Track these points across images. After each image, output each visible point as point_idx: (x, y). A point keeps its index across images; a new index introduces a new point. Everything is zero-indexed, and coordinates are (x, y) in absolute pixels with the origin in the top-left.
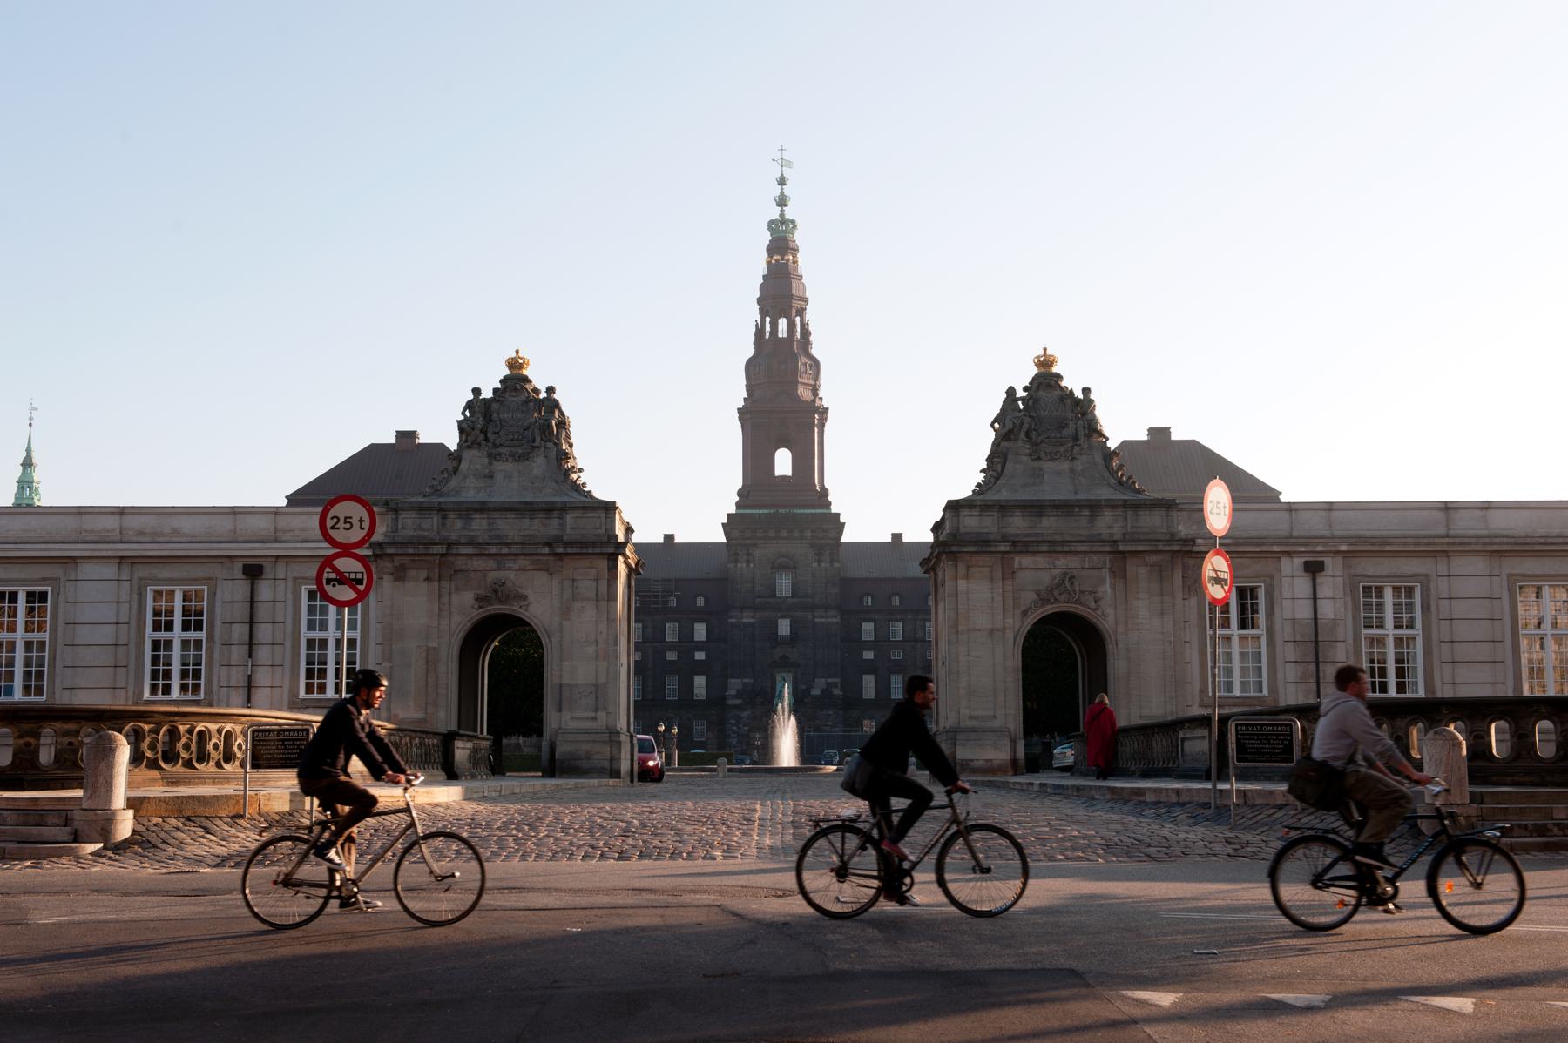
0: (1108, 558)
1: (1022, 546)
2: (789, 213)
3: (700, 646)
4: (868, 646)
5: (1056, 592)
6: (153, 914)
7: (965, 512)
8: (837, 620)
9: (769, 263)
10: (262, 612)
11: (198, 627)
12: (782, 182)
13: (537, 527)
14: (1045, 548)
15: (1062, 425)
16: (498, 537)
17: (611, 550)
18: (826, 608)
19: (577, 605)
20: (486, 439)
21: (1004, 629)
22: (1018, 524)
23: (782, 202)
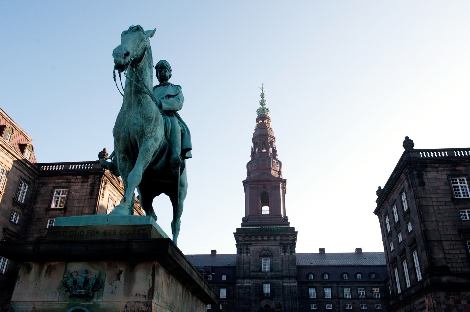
8: (296, 284)
9: (257, 125)
18: (290, 277)
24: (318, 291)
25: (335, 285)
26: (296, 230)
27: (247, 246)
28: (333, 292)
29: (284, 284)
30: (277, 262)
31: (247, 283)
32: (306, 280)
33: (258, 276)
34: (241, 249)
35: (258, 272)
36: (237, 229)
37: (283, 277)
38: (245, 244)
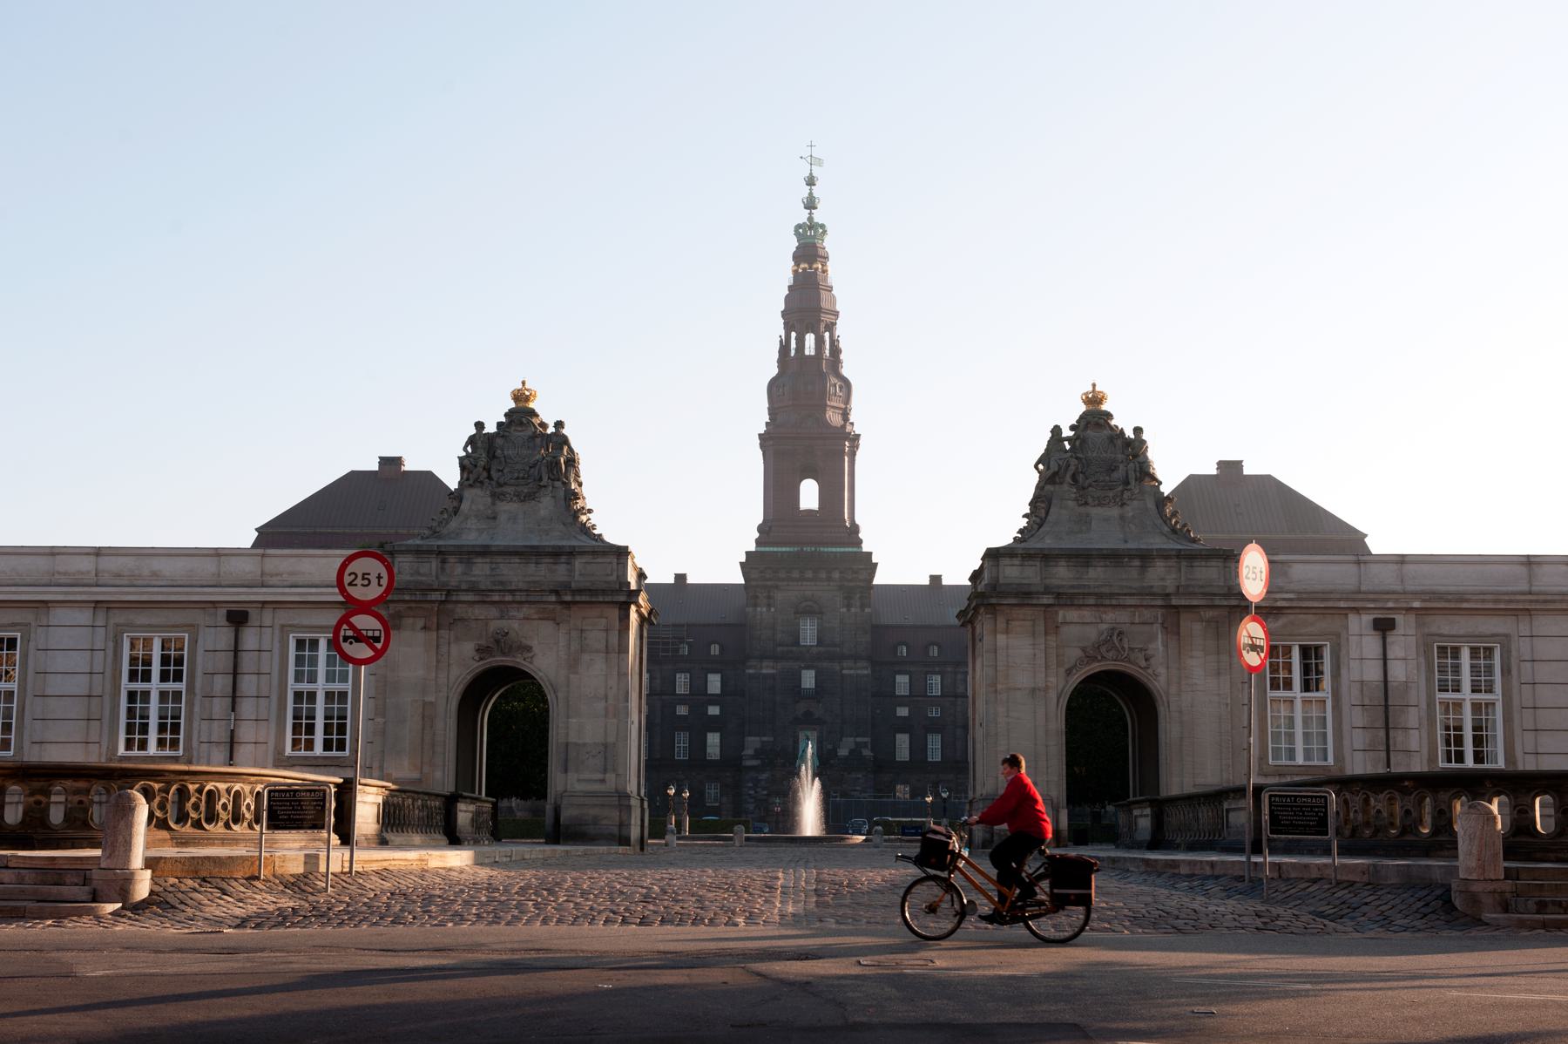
0: (1160, 612)
1: (1065, 598)
2: (818, 217)
3: (714, 700)
4: (902, 701)
5: (1103, 649)
6: (195, 968)
7: (1006, 561)
9: (795, 272)
10: (247, 662)
11: (178, 677)
12: (811, 181)
13: (542, 573)
14: (1091, 601)
15: (1112, 469)
16: (501, 583)
17: (622, 598)
18: (856, 658)
19: (586, 657)
20: (490, 477)
21: (1046, 689)
22: (1062, 574)
23: (810, 204)
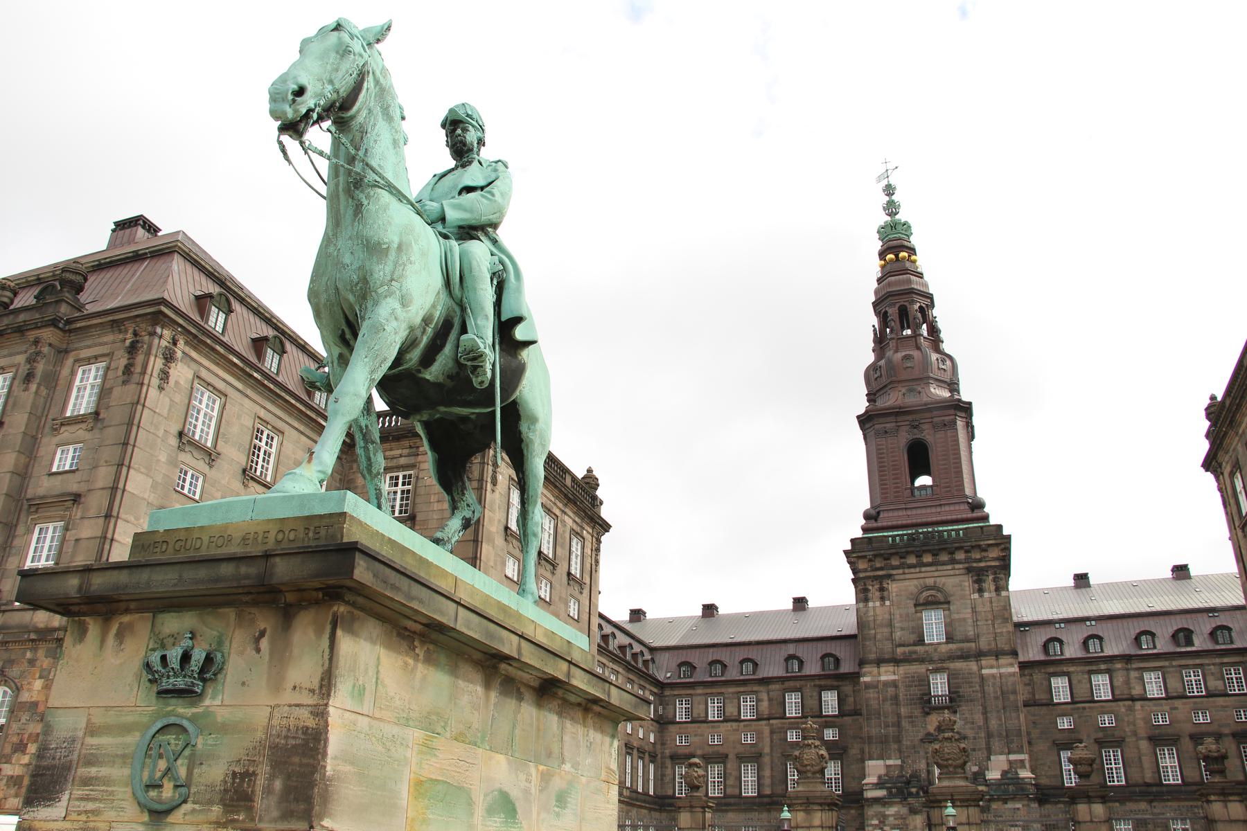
3: (829, 722)
9: (883, 267)
18: (998, 654)
24: (1074, 682)
25: (1119, 666)
26: (1005, 533)
27: (881, 583)
28: (1116, 684)
29: (984, 671)
30: (962, 616)
31: (887, 674)
32: (1042, 657)
33: (914, 656)
34: (866, 590)
35: (915, 644)
36: (853, 541)
37: (979, 655)
38: (876, 578)
